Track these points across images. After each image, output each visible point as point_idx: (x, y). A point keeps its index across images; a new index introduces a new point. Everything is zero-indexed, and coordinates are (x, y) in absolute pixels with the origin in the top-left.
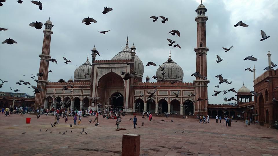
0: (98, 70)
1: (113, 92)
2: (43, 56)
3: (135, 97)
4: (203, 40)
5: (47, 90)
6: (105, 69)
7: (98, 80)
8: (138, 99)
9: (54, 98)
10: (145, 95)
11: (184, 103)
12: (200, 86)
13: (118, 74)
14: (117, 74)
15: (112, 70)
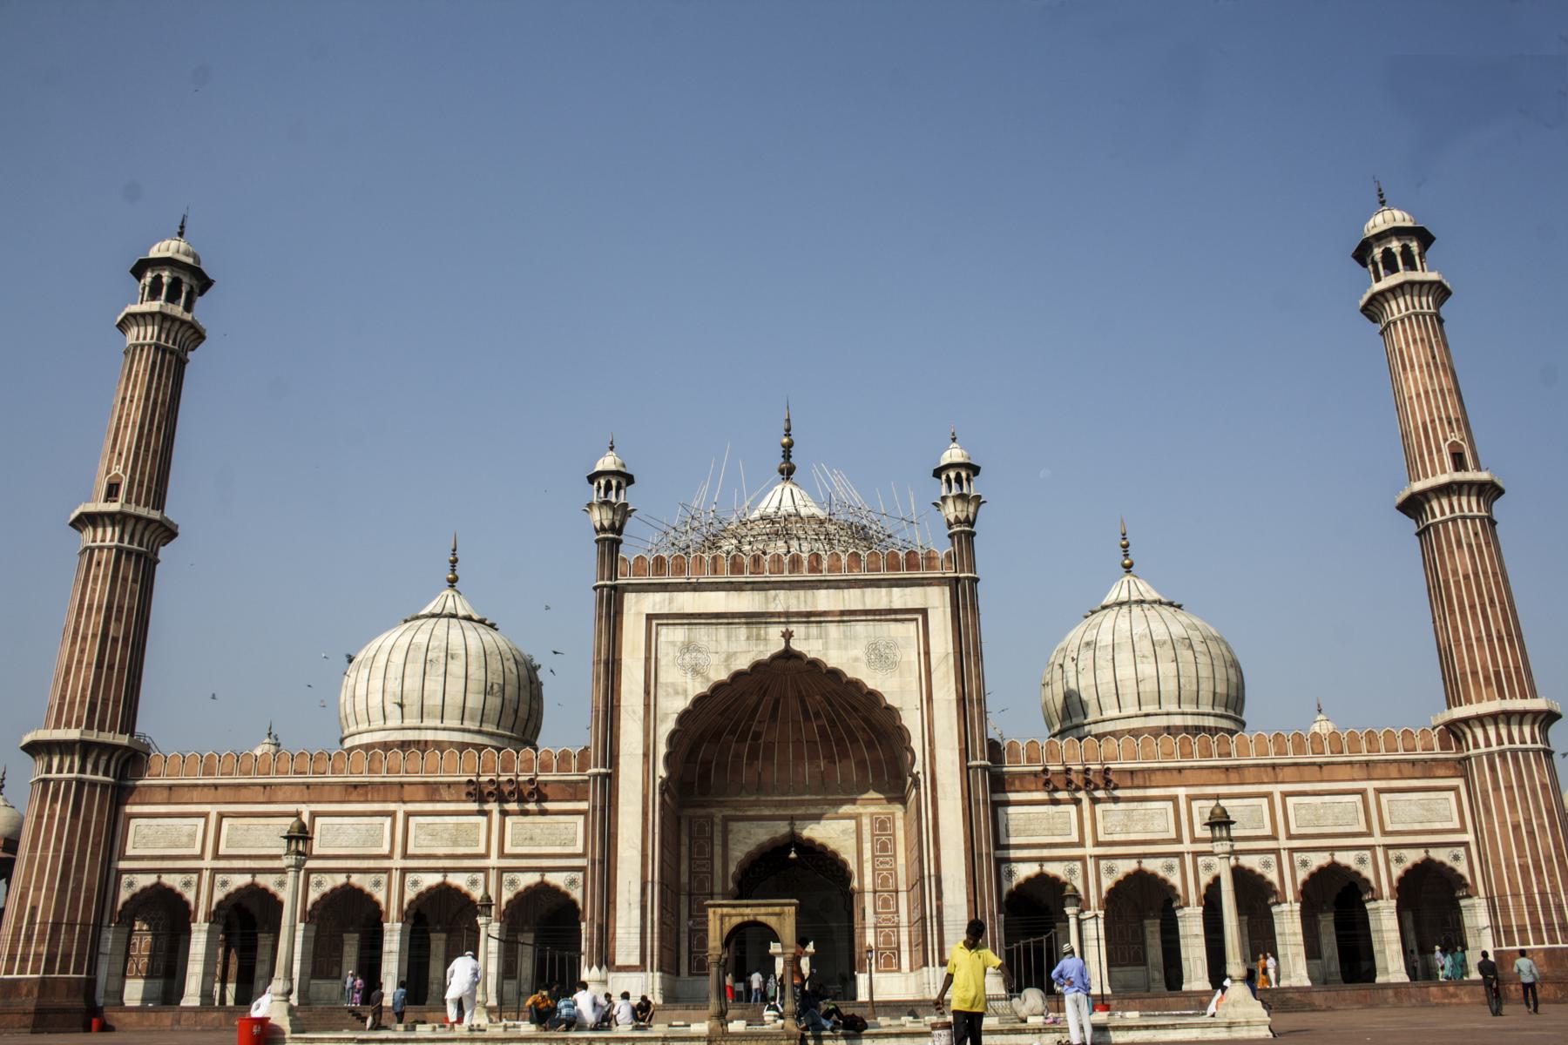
0: (662, 639)
1: (750, 837)
2: (112, 518)
3: (1004, 867)
4: (1459, 429)
5: (134, 823)
6: (722, 631)
7: (666, 727)
8: (1029, 880)
9: (202, 897)
10: (1089, 841)
11: (1399, 890)
12: (1518, 745)
13: (849, 676)
14: (836, 674)
15: (788, 636)
